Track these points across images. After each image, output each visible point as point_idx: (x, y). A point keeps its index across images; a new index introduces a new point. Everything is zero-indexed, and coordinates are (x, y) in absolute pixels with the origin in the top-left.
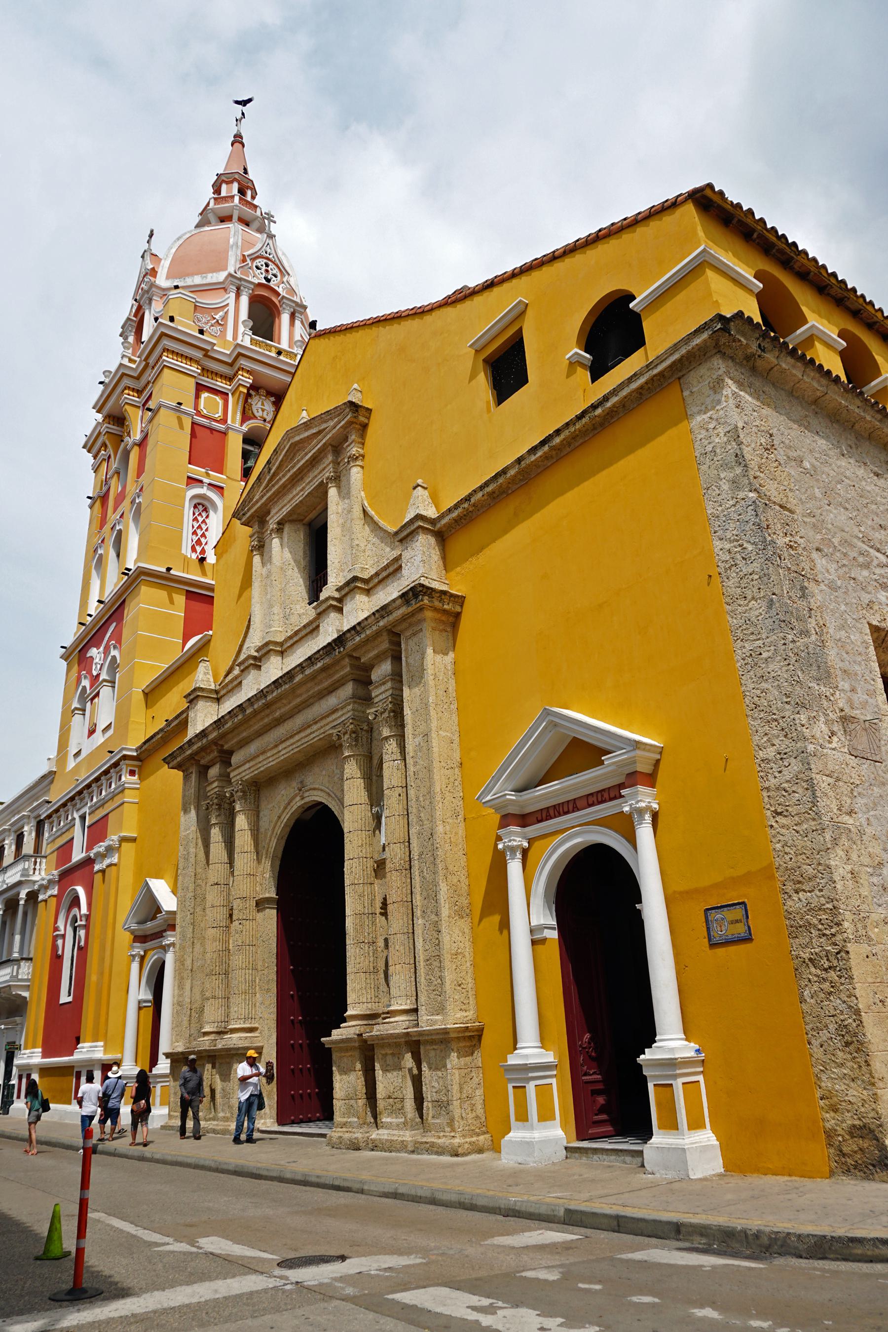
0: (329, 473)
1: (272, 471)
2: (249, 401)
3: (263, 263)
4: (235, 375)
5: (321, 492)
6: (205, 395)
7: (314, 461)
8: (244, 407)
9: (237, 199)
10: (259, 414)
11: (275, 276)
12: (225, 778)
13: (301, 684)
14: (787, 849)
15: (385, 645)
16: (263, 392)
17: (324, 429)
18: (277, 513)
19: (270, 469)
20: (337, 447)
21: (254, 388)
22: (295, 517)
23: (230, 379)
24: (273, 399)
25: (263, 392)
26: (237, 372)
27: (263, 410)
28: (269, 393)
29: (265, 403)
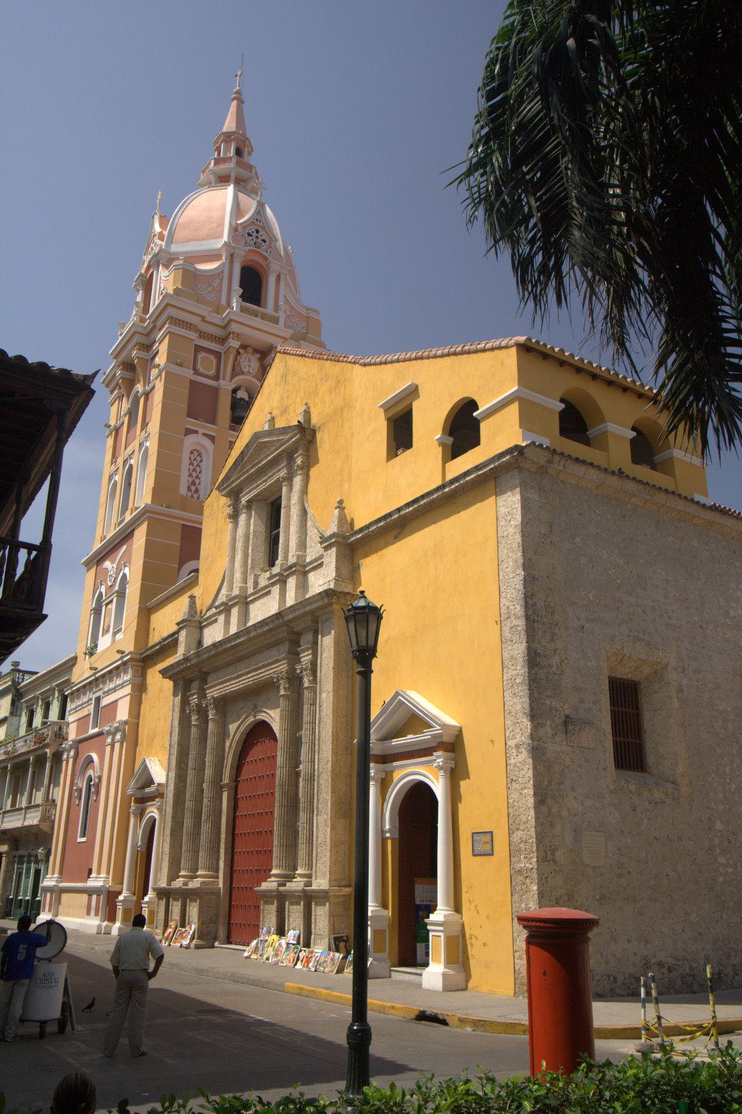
0: (283, 473)
1: (245, 459)
2: (239, 358)
3: (254, 230)
4: (227, 337)
5: (277, 486)
6: (202, 355)
7: (274, 462)
8: (234, 364)
9: (234, 161)
10: (245, 370)
11: (264, 241)
12: (202, 695)
13: (255, 637)
14: (515, 804)
15: (309, 623)
16: (250, 350)
17: (282, 439)
18: (247, 493)
19: (243, 458)
20: (290, 455)
21: (244, 347)
22: (260, 497)
23: (222, 341)
24: (258, 356)
25: (250, 350)
26: (229, 335)
27: (249, 366)
28: (256, 351)
29: (252, 360)
